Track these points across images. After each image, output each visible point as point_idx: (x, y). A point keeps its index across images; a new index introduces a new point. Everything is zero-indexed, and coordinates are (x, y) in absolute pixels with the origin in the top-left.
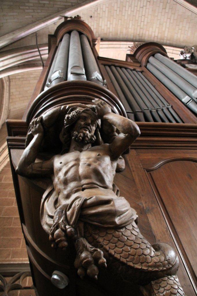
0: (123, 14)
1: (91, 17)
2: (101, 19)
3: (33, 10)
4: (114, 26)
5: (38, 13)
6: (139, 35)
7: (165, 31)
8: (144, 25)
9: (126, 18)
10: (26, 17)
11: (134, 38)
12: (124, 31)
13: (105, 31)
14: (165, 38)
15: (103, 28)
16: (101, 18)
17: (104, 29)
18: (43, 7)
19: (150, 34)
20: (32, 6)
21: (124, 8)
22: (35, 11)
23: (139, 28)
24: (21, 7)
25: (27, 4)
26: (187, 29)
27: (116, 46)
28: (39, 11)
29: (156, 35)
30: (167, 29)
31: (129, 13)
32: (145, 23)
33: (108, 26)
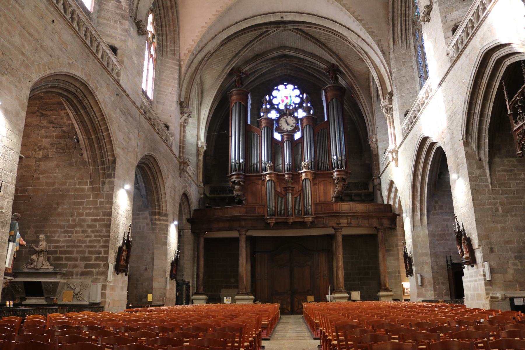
5: (219, 66)
10: (214, 72)
28: (219, 65)
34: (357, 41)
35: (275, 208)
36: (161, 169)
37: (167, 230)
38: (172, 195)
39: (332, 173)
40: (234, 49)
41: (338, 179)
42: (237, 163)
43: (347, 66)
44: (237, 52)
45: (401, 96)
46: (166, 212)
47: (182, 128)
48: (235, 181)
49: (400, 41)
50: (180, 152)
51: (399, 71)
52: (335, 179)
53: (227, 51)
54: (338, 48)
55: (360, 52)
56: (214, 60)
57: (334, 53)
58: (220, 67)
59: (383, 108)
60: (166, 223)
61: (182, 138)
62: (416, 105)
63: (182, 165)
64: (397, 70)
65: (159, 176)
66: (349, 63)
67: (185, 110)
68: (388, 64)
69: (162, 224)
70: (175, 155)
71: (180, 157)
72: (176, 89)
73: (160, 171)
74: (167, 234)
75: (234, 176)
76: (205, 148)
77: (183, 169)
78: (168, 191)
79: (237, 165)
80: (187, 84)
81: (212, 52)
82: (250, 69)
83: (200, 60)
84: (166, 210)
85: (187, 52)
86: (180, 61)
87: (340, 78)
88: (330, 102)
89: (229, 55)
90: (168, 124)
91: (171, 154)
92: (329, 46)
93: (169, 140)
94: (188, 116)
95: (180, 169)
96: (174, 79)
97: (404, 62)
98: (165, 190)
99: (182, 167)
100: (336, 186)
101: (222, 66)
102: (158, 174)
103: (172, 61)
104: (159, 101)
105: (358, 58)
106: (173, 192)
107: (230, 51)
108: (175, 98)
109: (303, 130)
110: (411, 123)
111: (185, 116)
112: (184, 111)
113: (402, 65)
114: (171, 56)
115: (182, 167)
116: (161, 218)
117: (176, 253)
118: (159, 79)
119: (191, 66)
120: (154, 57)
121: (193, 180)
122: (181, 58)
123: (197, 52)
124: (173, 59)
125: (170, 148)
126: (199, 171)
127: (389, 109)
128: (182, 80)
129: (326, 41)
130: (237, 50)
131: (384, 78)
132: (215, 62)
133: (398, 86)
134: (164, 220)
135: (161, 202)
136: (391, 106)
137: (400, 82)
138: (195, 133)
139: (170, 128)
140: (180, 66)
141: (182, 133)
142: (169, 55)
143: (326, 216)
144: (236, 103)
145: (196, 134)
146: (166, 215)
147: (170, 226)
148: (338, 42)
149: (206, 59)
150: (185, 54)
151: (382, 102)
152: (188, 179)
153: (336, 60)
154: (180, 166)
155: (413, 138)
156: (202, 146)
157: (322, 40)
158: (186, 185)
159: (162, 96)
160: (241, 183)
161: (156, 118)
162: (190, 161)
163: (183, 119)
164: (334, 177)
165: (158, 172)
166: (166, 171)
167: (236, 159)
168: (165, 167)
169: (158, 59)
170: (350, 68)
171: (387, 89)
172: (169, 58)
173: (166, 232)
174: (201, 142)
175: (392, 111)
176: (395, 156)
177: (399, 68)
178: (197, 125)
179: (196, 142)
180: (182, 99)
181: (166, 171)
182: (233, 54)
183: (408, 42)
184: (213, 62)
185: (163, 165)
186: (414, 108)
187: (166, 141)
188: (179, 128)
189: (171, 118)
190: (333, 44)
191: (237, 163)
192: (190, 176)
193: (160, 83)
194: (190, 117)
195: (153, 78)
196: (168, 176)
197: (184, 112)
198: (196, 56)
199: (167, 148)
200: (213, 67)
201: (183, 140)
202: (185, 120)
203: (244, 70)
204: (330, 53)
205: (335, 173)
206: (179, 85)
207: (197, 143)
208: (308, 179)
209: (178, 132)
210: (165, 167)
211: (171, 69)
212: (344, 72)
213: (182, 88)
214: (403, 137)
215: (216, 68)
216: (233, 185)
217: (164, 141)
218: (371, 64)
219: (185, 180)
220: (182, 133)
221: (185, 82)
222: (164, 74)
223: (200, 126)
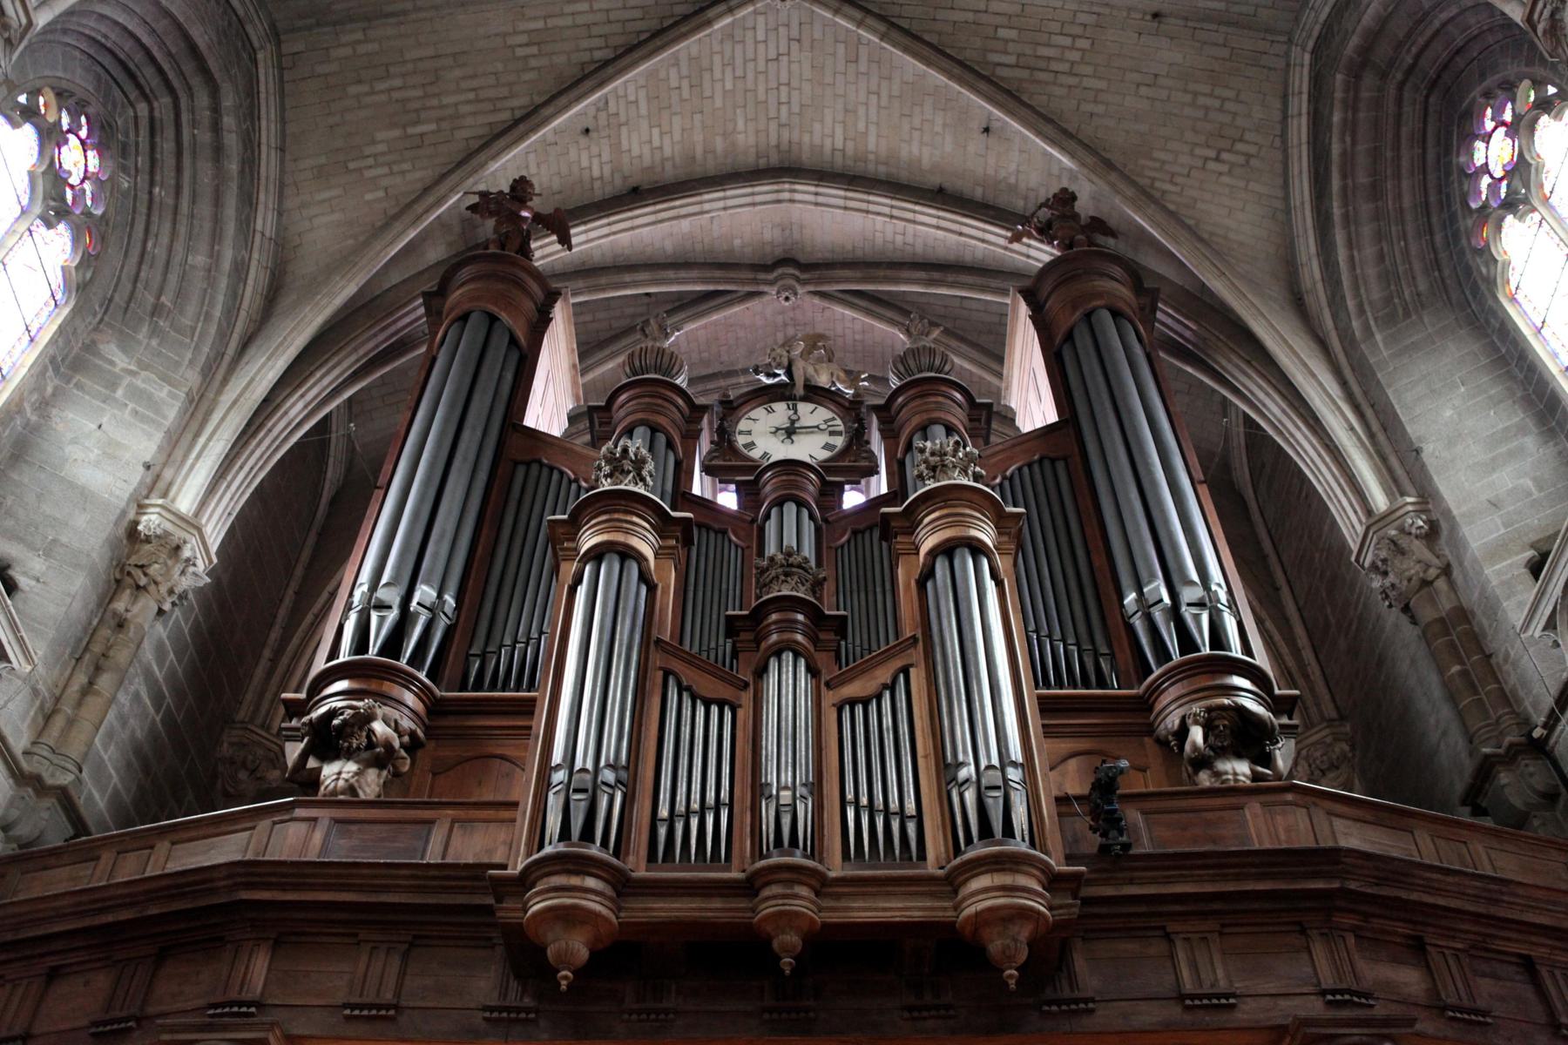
0: (707, 93)
1: (587, 131)
2: (624, 130)
3: (389, 164)
4: (677, 137)
5: (403, 173)
6: (778, 146)
7: (866, 134)
8: (790, 113)
9: (718, 103)
10: (368, 197)
11: (762, 163)
12: (719, 144)
13: (647, 161)
14: (871, 157)
15: (636, 151)
16: (626, 123)
17: (640, 157)
18: (418, 147)
19: (817, 141)
20: (383, 154)
21: (707, 76)
22: (396, 168)
23: (773, 126)
24: (352, 165)
25: (368, 151)
26: (938, 129)
27: (684, 211)
28: (406, 166)
29: (839, 144)
30: (872, 129)
31: (729, 86)
32: (796, 109)
33: (656, 143)
35: (629, 786)
39: (1145, 704)
40: (504, 91)
42: (382, 606)
48: (333, 713)
52: (1183, 732)
53: (462, 97)
54: (1088, 107)
56: (380, 136)
58: (409, 177)
66: (1158, 184)
79: (374, 617)
88: (1069, 337)
92: (1038, 101)
105: (1212, 154)
107: (478, 101)
109: (902, 464)
129: (1025, 74)
130: (521, 102)
132: (381, 148)
138: (145, 445)
143: (1197, 907)
144: (464, 318)
148: (1089, 70)
157: (1001, 72)
160: (378, 727)
164: (1173, 721)
170: (1171, 207)
182: (492, 118)
184: (374, 142)
190: (1058, 91)
200: (368, 174)
208: (977, 549)
215: (385, 182)
216: (312, 763)
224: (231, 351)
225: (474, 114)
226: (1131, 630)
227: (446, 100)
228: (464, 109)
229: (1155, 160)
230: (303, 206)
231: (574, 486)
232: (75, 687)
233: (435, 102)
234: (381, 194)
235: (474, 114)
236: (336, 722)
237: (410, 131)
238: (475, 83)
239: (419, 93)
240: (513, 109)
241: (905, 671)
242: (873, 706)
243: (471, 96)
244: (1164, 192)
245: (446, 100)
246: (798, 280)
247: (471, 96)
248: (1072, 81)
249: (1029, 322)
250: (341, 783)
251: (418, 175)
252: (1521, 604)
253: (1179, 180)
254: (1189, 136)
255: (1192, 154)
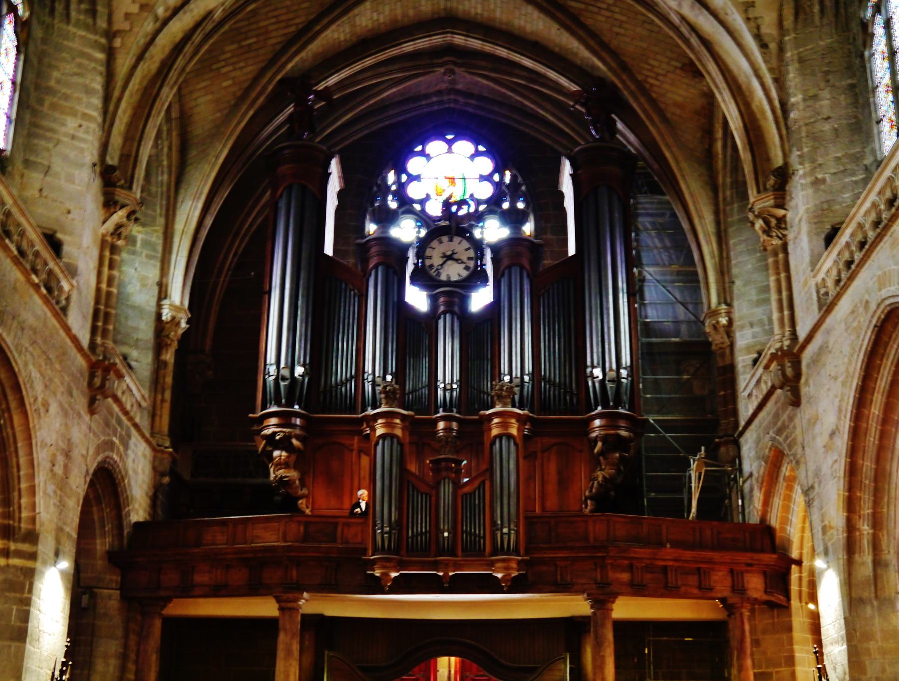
5: (240, 68)
10: (225, 84)
12: (411, 13)
13: (370, 26)
14: (498, 20)
20: (230, 58)
24: (214, 67)
28: (242, 64)
29: (479, 11)
34: (680, 5)
36: (21, 380)
37: (31, 591)
38: (59, 470)
40: (290, 16)
41: (605, 439)
42: (284, 379)
43: (643, 89)
44: (300, 26)
45: (816, 182)
46: (30, 527)
47: (107, 254)
48: (274, 433)
49: (816, 9)
50: (94, 330)
51: (810, 103)
54: (616, 30)
55: (687, 41)
57: (605, 46)
59: (757, 216)
60: (29, 564)
61: (104, 286)
62: (867, 204)
63: (99, 373)
64: (804, 100)
65: (13, 405)
67: (121, 195)
68: (776, 80)
69: (15, 567)
70: (75, 340)
71: (93, 345)
72: (94, 126)
73: (17, 388)
74: (28, 602)
75: (274, 420)
76: (184, 325)
77: (103, 385)
78: (42, 456)
79: (282, 384)
80: (129, 112)
81: (218, 15)
82: (340, 85)
83: (178, 39)
84: (33, 520)
85: (135, 9)
86: (110, 35)
87: (620, 125)
89: (274, 34)
90: (60, 236)
91: (62, 333)
92: (589, 22)
93: (61, 289)
94: (128, 216)
95: (90, 384)
96: (89, 91)
97: (827, 73)
98: (31, 454)
99: (98, 381)
100: (599, 464)
101: (251, 69)
102: (11, 397)
103: (84, 34)
104: (32, 158)
106: (61, 460)
108: (90, 154)
110: (849, 264)
111: (119, 216)
112: (117, 198)
113: (822, 85)
114: (82, 17)
115: (98, 381)
116: (13, 546)
117: (59, 667)
118: (38, 87)
119: (147, 55)
120: (21, 13)
121: (136, 426)
122: (116, 27)
123: (169, 13)
124: (87, 28)
125: (61, 312)
126: (159, 397)
127: (773, 222)
128: (114, 100)
131: (762, 123)
132: (228, 55)
133: (805, 150)
134: (20, 554)
135: (16, 494)
136: (780, 212)
137: (815, 138)
138: (153, 274)
139: (66, 249)
140: (111, 54)
141: (106, 270)
142: (74, 14)
145: (157, 279)
146: (32, 537)
147: (43, 573)
148: (617, 10)
149: (197, 38)
150: (127, 16)
151: (752, 200)
152: (120, 422)
153: (610, 68)
154: (92, 376)
155: (853, 312)
156: (173, 318)
158: (112, 443)
159: (43, 143)
160: (295, 442)
161: (15, 211)
162: (133, 364)
163: (110, 225)
164: (594, 434)
165: (9, 392)
166: (39, 387)
167: (282, 365)
168: (35, 374)
169: (35, 22)
170: (654, 95)
171: (768, 159)
172: (73, 21)
173: (26, 595)
174: (172, 306)
175: (785, 229)
176: (789, 371)
177: (811, 93)
178: (160, 249)
179: (153, 302)
180: (113, 159)
181: (39, 387)
182: (286, 31)
183: (842, 11)
184: (224, 53)
185: (31, 367)
186: (859, 217)
187: (50, 287)
188: (95, 253)
189: (70, 216)
191: (284, 379)
192: (126, 413)
193: (41, 102)
194: (137, 219)
195: (14, 83)
196: (46, 406)
197: (116, 203)
198: (166, 22)
199: (49, 314)
201: (109, 294)
202: (119, 226)
203: (321, 87)
204: (592, 43)
205: (597, 422)
206: (105, 112)
207: (159, 306)
209: (93, 264)
210: (35, 374)
211: (78, 60)
212: (635, 105)
213: (112, 124)
214: (820, 309)
215: (233, 74)
217: (37, 287)
218: (719, 79)
219: (107, 424)
220: (106, 270)
221: (123, 105)
222: (56, 74)
223: (170, 253)
224: (172, 194)
225: (277, 30)
226: (587, 383)
227: (262, 24)
228: (271, 28)
229: (649, 65)
230: (191, 93)
231: (352, 293)
232: (159, 402)
233: (254, 27)
234: (229, 82)
235: (277, 30)
236: (277, 437)
237: (244, 43)
238: (275, 13)
239: (246, 23)
240: (297, 25)
241: (484, 482)
242: (473, 496)
243: (274, 20)
244: (652, 85)
245: (262, 24)
246: (455, 64)
247: (274, 20)
248: (608, 14)
249: (570, 178)
250: (282, 461)
251: (249, 69)
252: (745, 380)
253: (661, 78)
254: (669, 54)
255: (668, 64)
